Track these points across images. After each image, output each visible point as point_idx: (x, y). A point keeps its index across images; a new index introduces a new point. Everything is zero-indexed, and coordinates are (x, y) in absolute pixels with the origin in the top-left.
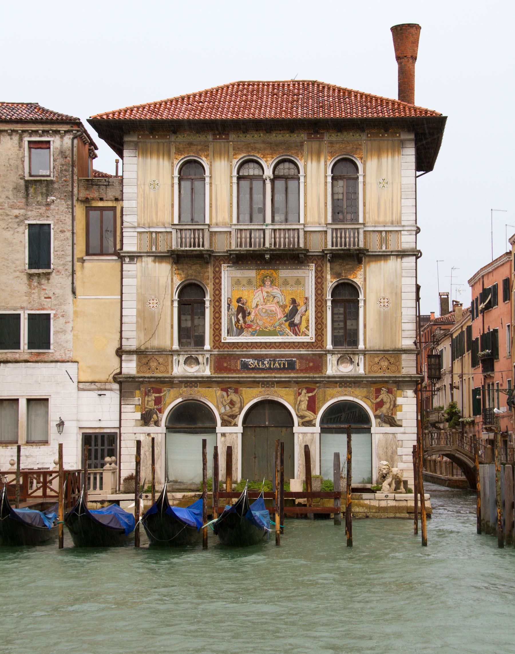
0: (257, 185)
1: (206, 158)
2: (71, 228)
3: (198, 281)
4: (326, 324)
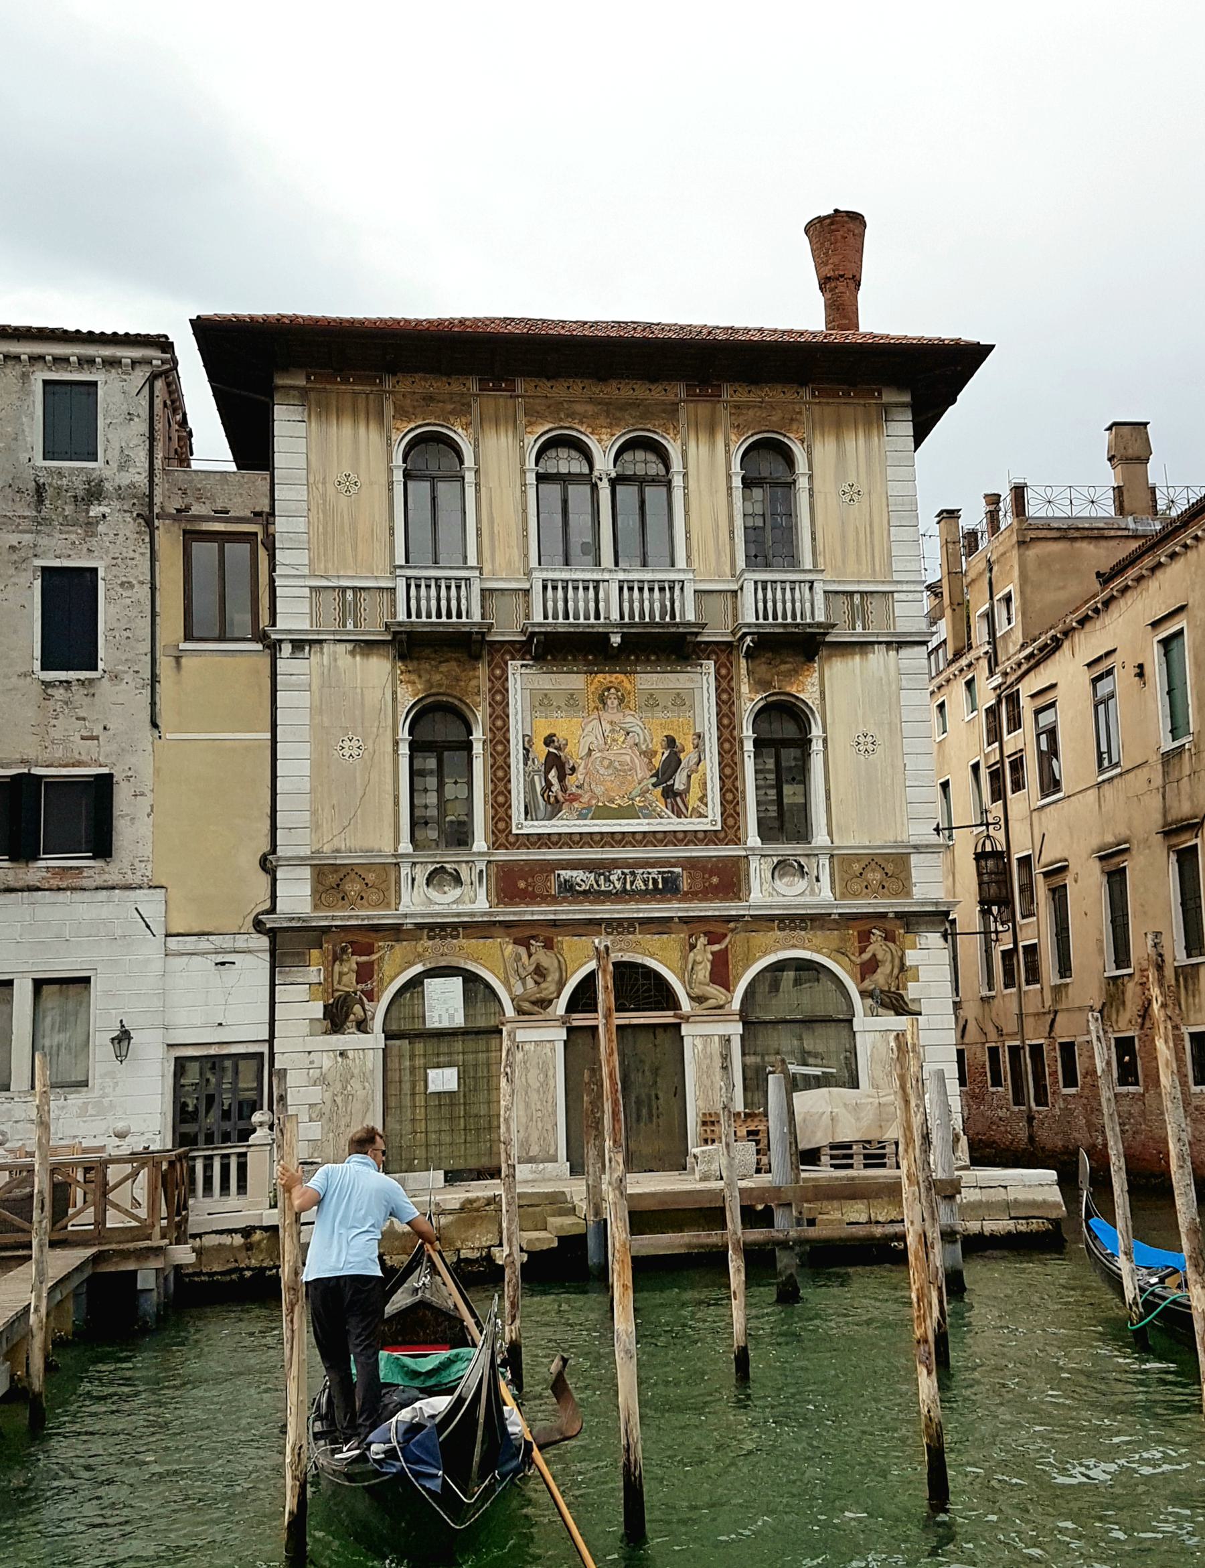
0: (579, 494)
3: (455, 697)
4: (744, 792)
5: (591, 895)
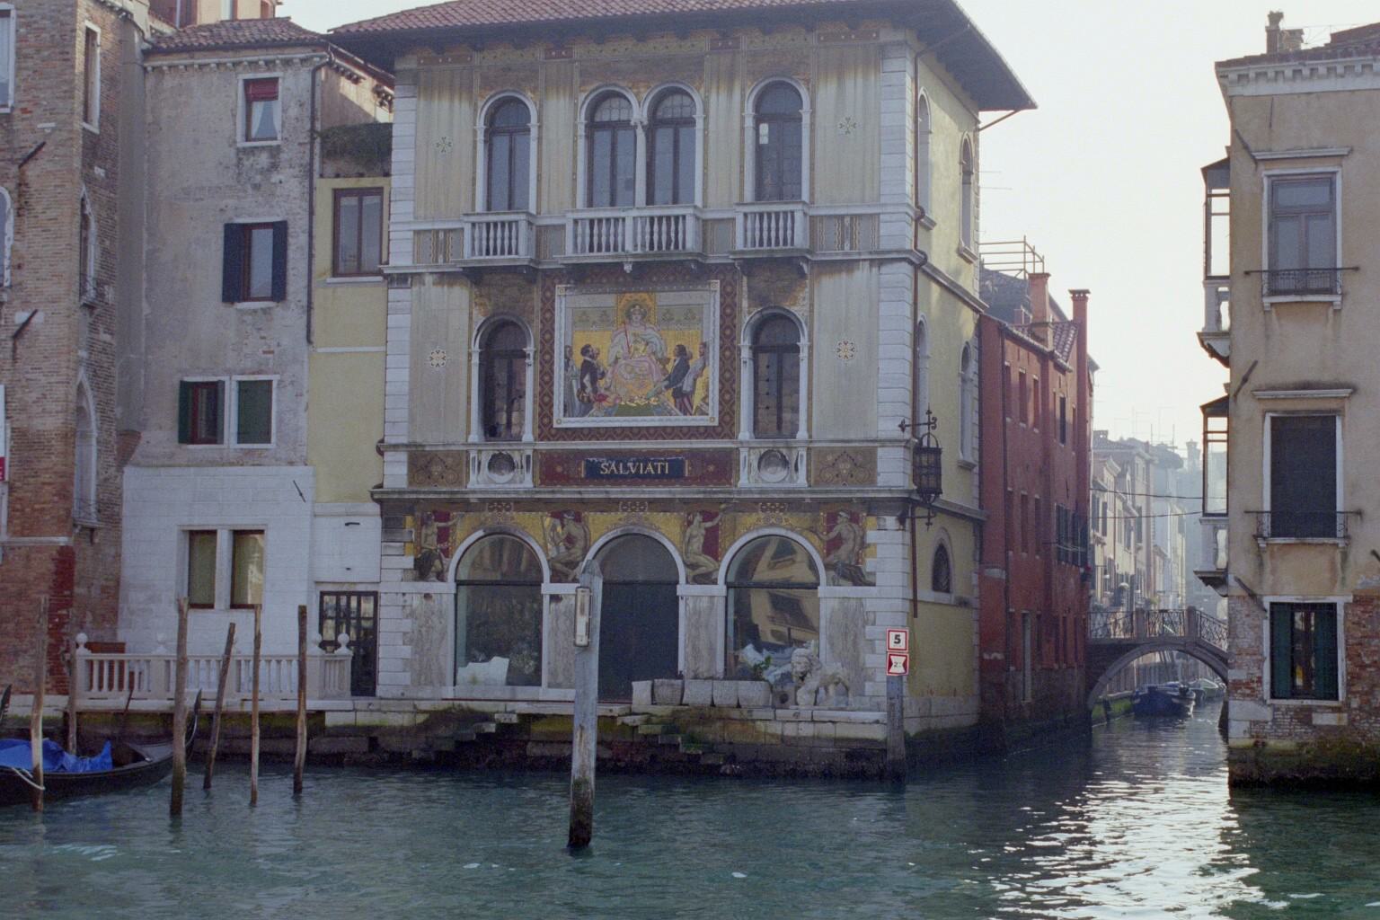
0: (622, 135)
1: (533, 92)
2: (307, 227)
5: (614, 479)
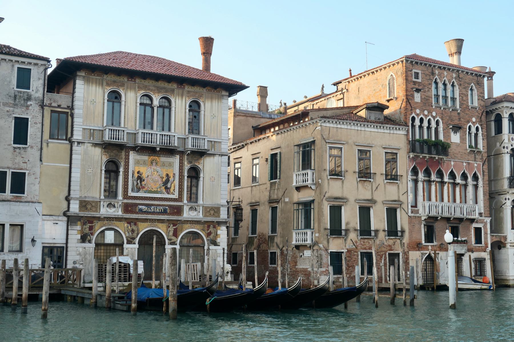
2: (41, 122)
